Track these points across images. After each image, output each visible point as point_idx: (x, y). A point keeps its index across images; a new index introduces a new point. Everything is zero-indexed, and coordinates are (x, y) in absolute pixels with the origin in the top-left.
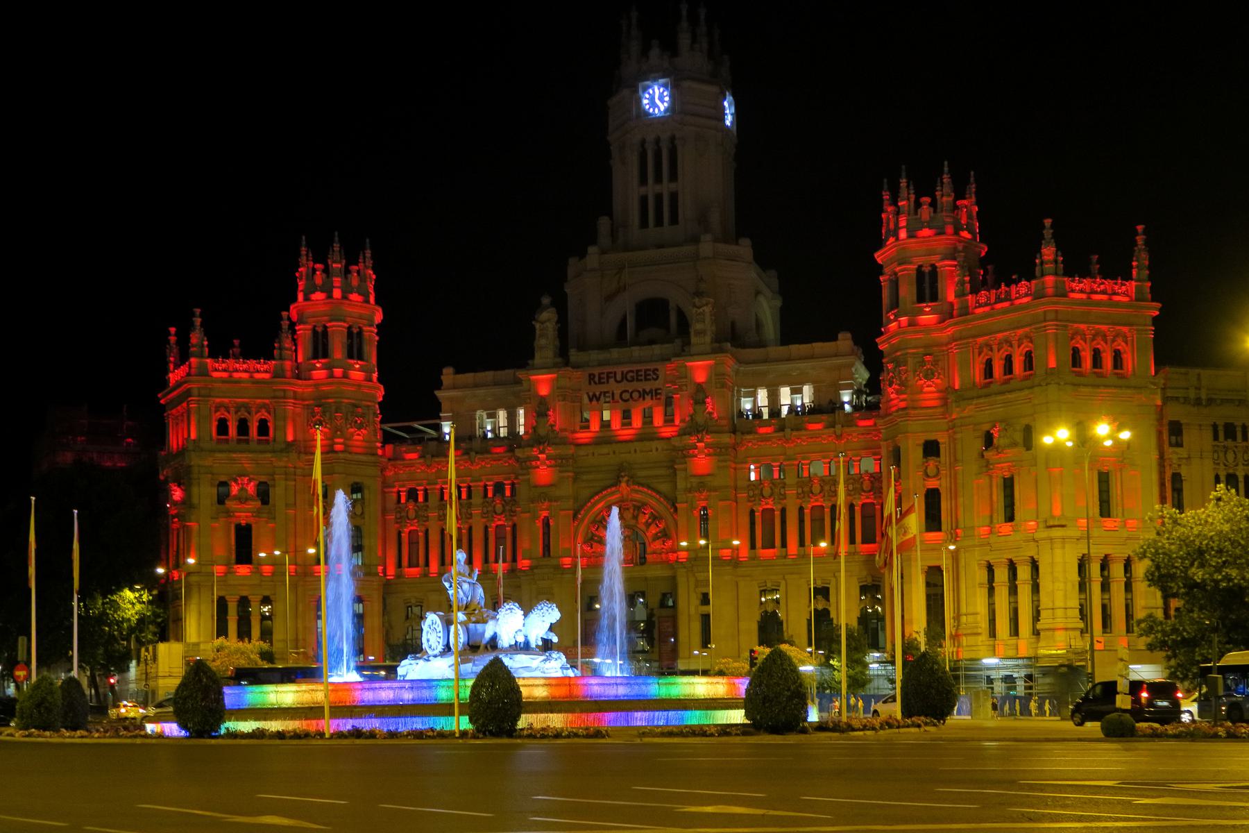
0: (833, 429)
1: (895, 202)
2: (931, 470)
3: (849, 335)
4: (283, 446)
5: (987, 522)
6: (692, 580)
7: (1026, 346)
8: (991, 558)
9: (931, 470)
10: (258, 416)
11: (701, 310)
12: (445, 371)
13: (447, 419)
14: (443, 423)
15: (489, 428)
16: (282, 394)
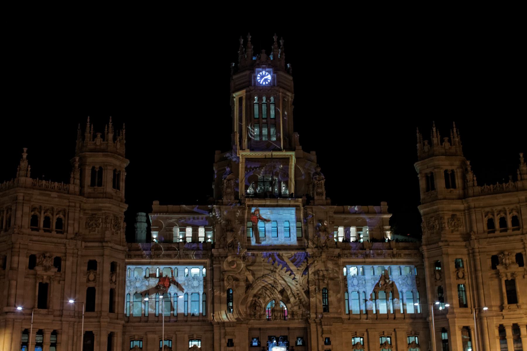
0: (391, 251)
1: (427, 136)
2: (460, 275)
3: (386, 203)
4: (73, 236)
5: (498, 303)
6: (320, 330)
7: (515, 213)
8: (504, 322)
9: (460, 275)
10: (58, 216)
11: (320, 182)
12: (154, 202)
13: (155, 230)
14: (152, 232)
15: (181, 237)
16: (73, 204)
